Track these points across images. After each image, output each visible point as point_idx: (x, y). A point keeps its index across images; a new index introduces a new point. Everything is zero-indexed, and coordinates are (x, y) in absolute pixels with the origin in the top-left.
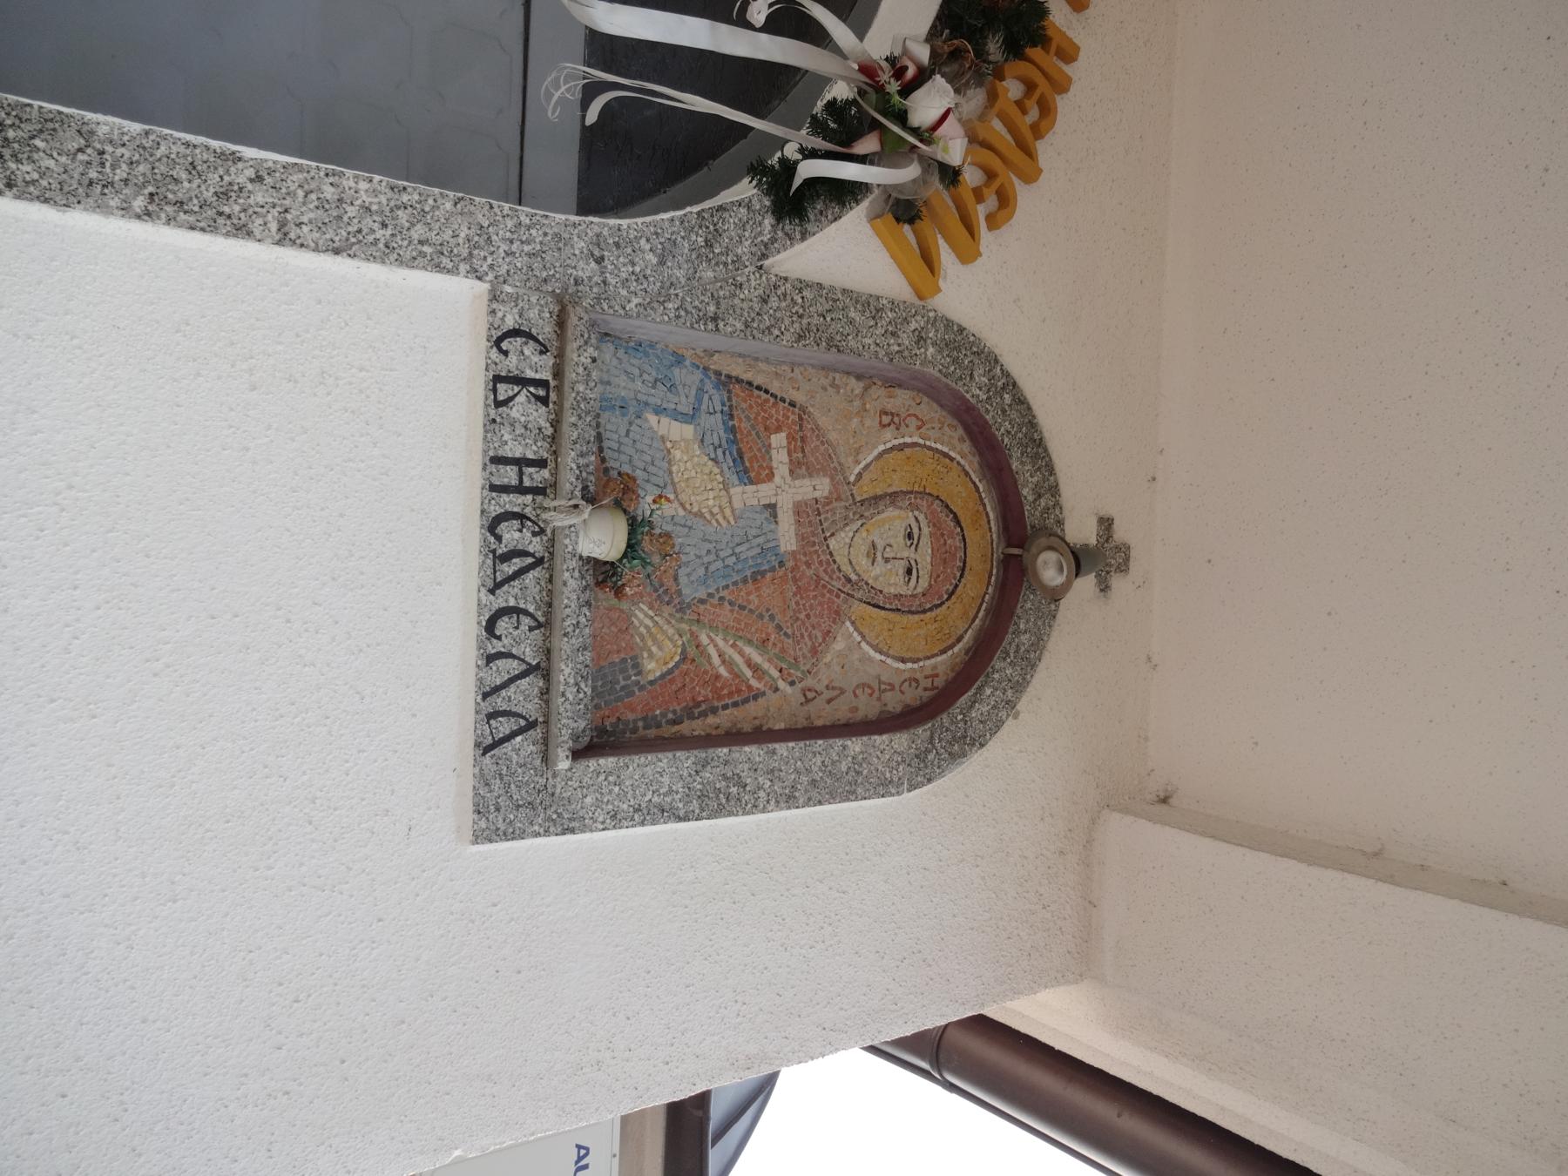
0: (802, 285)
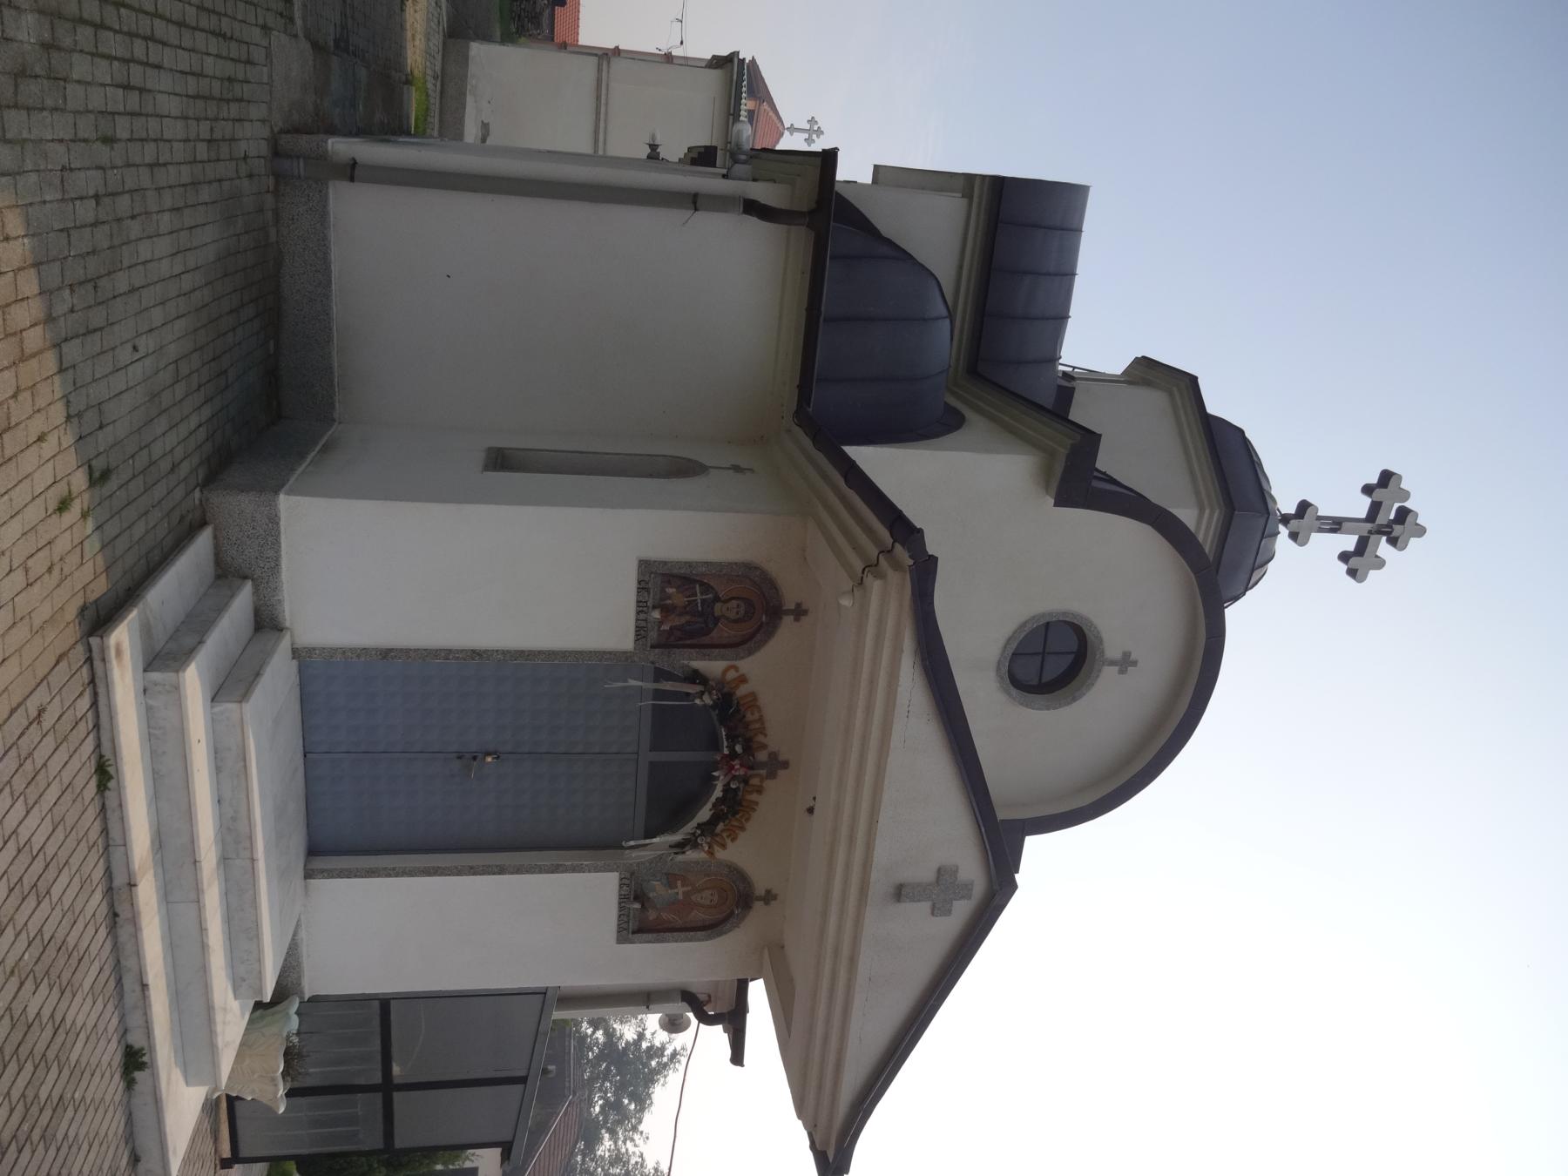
0: (680, 862)
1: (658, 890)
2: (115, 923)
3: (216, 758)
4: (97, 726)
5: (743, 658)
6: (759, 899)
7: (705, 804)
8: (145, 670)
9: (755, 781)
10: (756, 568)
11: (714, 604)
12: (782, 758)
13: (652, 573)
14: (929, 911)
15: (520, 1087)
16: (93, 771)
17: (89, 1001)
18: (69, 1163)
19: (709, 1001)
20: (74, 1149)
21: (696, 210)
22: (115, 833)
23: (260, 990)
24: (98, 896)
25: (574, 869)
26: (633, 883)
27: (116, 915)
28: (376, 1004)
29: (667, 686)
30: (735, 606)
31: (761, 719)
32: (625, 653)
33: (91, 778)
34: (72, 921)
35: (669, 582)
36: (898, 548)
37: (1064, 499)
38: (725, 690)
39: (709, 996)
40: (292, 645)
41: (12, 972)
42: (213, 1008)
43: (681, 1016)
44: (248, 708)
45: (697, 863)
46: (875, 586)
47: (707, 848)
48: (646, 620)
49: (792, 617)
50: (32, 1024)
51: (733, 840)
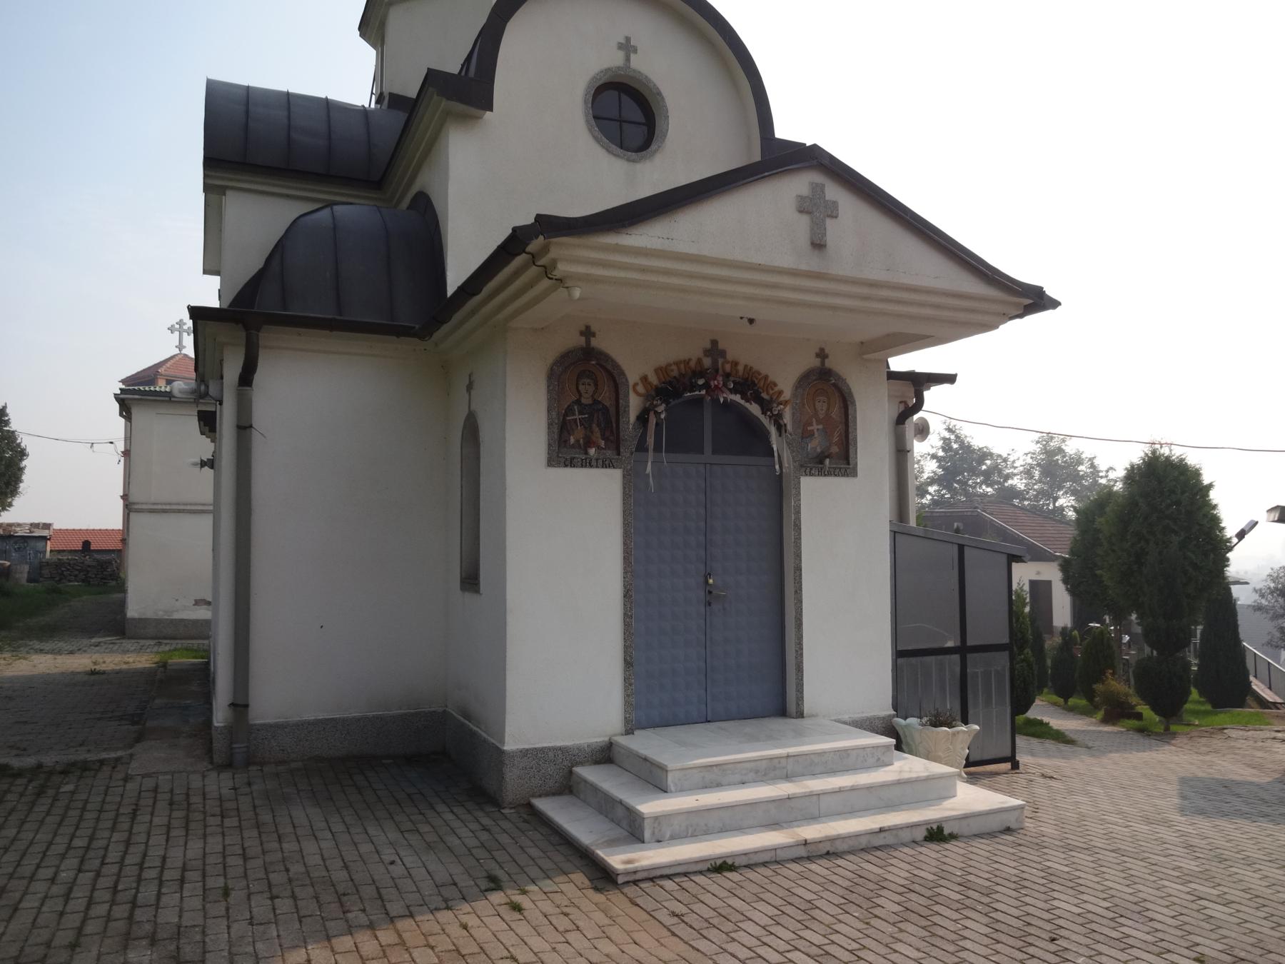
1: (815, 445)
2: (833, 853)
3: (710, 787)
4: (685, 874)
5: (627, 380)
6: (823, 363)
7: (746, 409)
8: (643, 842)
9: (728, 368)
10: (552, 369)
11: (583, 404)
12: (708, 346)
13: (558, 456)
14: (834, 219)
15: (967, 551)
16: (720, 875)
17: (890, 869)
18: (1008, 877)
19: (905, 403)
20: (997, 873)
21: (251, 426)
22: (766, 857)
23: (887, 747)
24: (813, 867)
25: (798, 512)
26: (809, 465)
27: (828, 853)
28: (900, 661)
29: (651, 441)
30: (583, 387)
31: (677, 363)
32: (624, 476)
33: (725, 877)
34: (832, 884)
35: (566, 441)
36: (530, 248)
37: (486, 103)
38: (653, 393)
39: (901, 402)
40: (622, 735)
41: (867, 923)
42: (899, 780)
43: (916, 424)
44: (671, 765)
45: (793, 414)
46: (562, 268)
47: (782, 406)
48: (597, 460)
49: (592, 339)
50: (905, 908)
51: (775, 385)
